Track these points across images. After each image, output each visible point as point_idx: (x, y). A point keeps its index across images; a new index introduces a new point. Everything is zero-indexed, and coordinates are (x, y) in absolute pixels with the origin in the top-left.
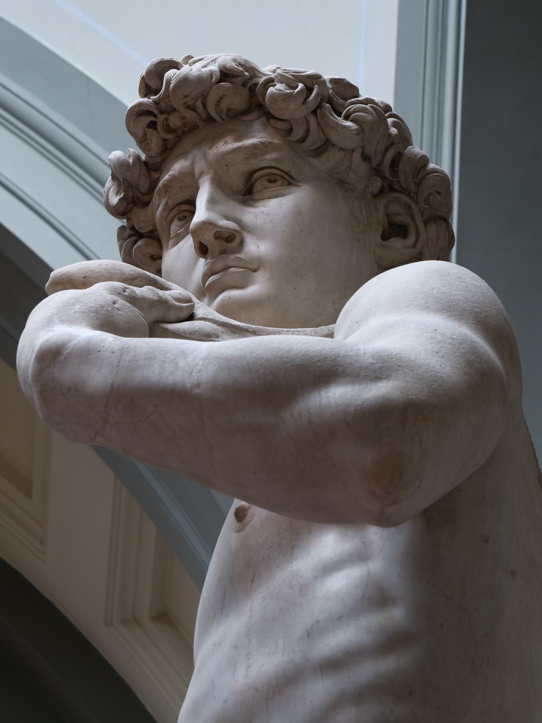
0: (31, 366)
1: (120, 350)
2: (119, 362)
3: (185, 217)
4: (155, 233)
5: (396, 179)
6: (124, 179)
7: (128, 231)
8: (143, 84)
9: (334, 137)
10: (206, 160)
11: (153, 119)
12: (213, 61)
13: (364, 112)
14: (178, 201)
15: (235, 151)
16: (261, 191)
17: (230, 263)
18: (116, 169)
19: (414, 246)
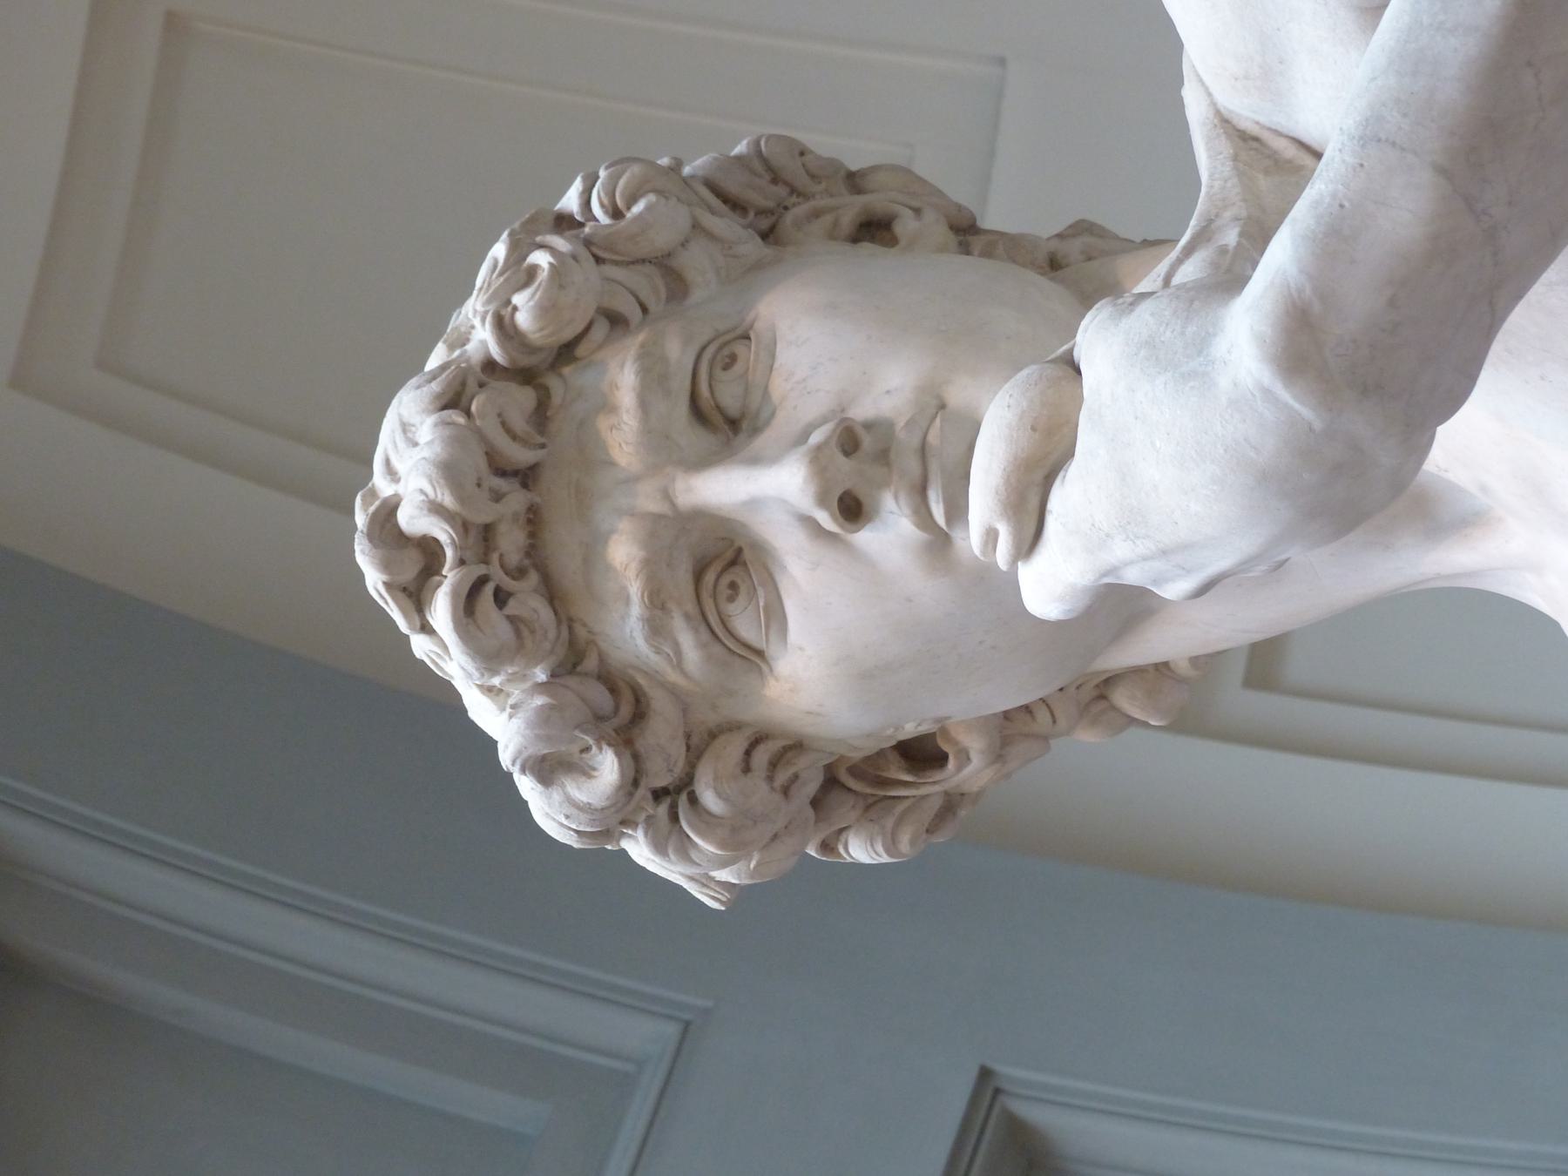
0: (1297, 406)
1: (1363, 146)
2: (1394, 144)
3: (733, 586)
4: (695, 740)
5: (751, 214)
6: (577, 727)
7: (662, 810)
8: (401, 595)
9: (661, 239)
10: (637, 479)
11: (489, 590)
12: (405, 427)
13: (619, 177)
14: (690, 588)
15: (644, 404)
16: (747, 391)
17: (915, 442)
18: (548, 739)
19: (917, 211)
